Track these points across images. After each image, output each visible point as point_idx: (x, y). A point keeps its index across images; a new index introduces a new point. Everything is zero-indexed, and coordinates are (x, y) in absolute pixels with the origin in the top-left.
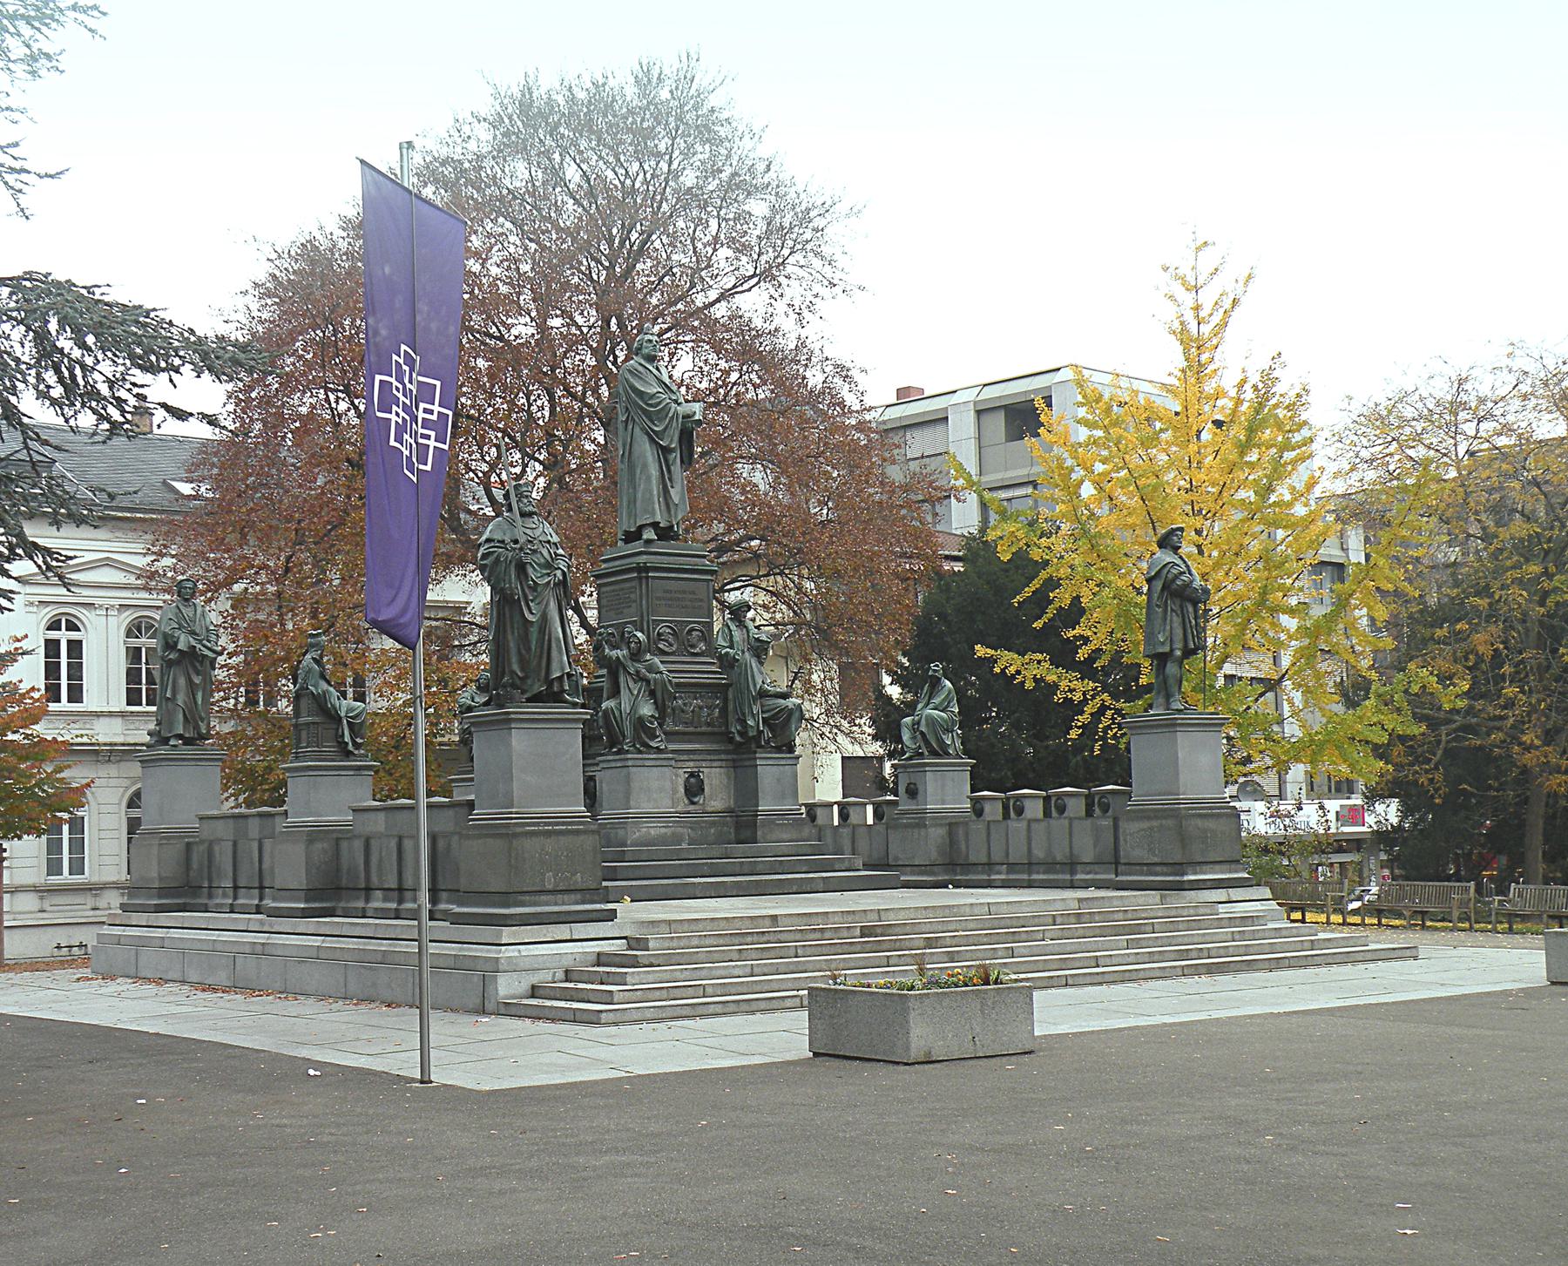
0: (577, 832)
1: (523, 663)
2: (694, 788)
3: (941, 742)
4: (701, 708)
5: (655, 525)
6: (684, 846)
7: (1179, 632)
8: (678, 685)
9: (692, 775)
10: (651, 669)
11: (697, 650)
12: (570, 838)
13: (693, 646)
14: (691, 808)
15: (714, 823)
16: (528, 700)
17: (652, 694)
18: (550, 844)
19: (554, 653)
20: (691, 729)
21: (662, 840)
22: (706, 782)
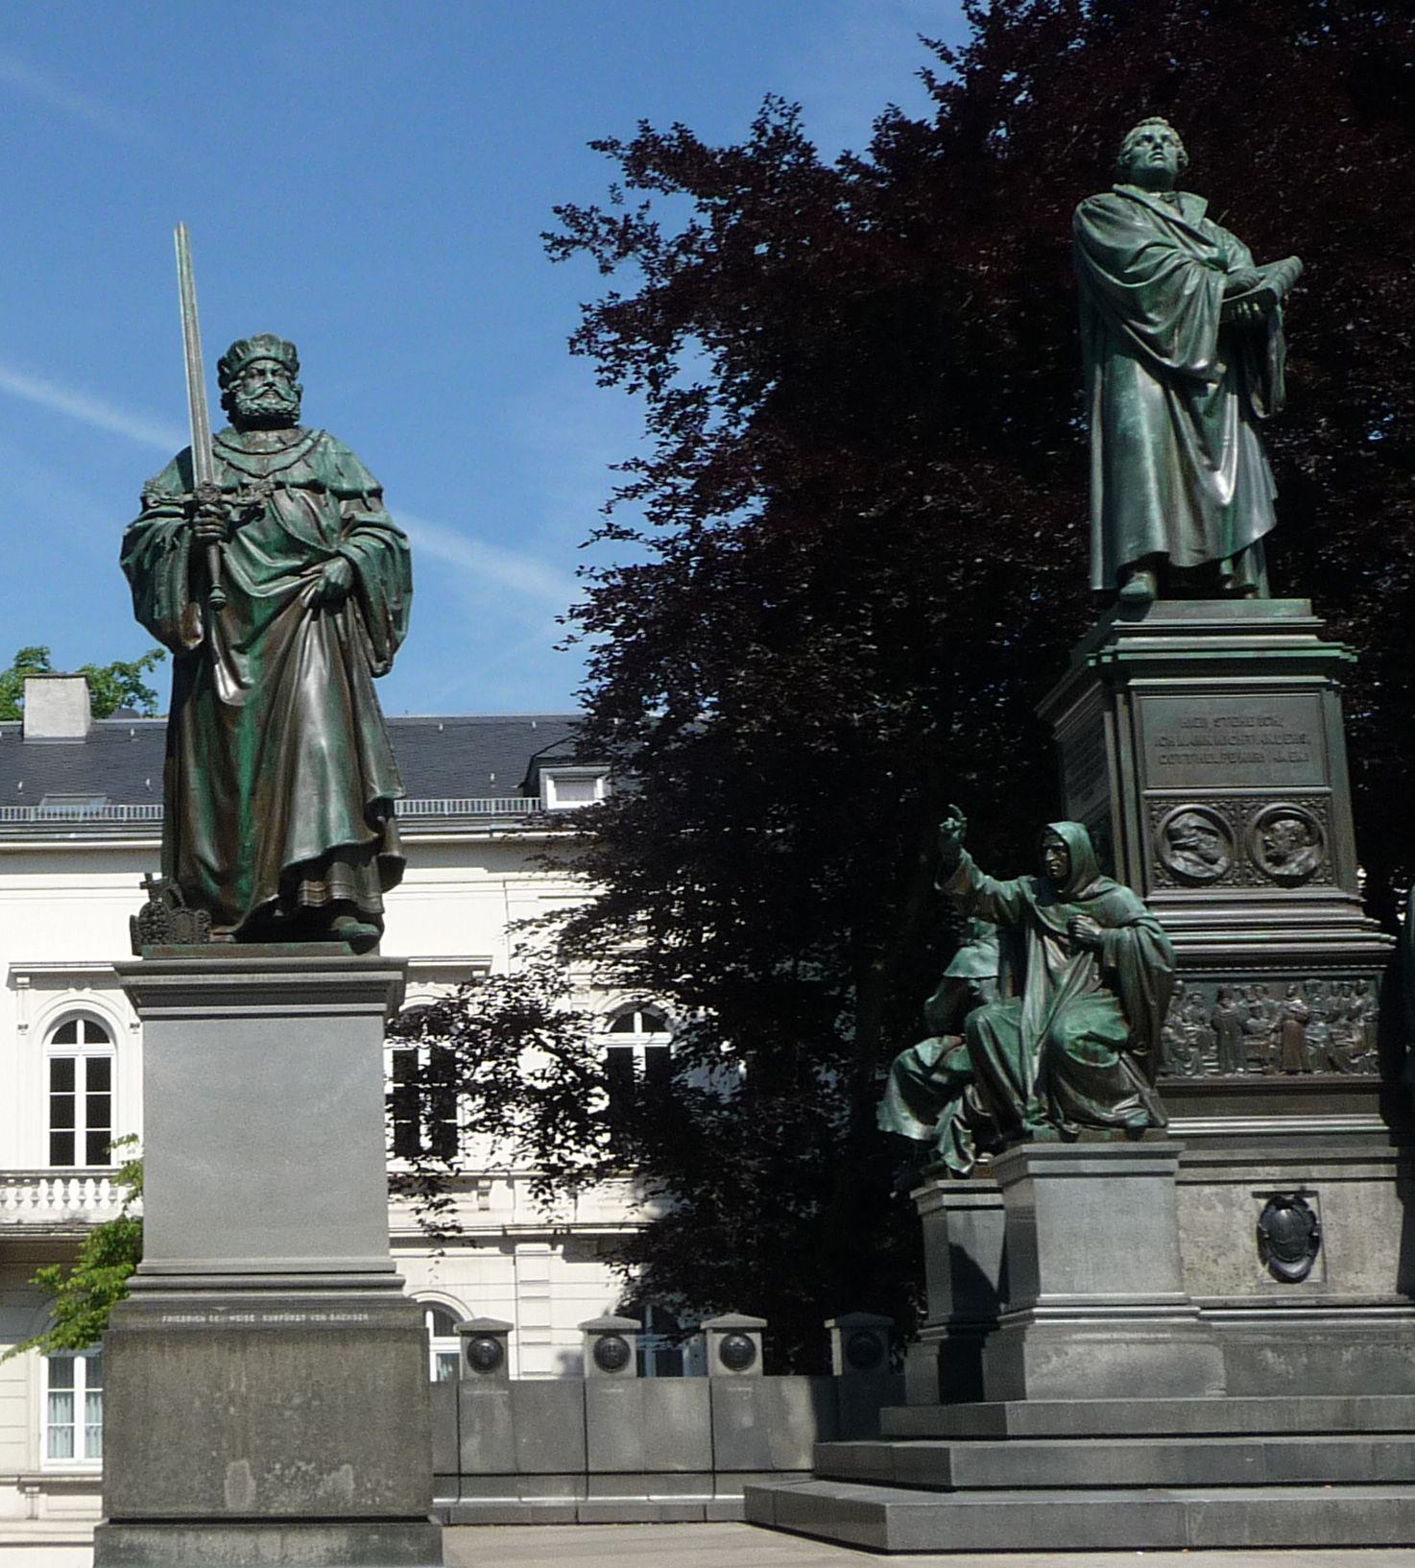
0: (344, 1334)
1: (225, 829)
2: (1288, 1239)
4: (1305, 1021)
5: (1157, 563)
6: (1213, 1394)
8: (1185, 961)
9: (1276, 1200)
10: (1109, 918)
11: (1292, 869)
12: (314, 1352)
13: (1279, 860)
14: (1283, 1292)
15: (1351, 1336)
16: (241, 937)
17: (1111, 980)
18: (241, 1371)
19: (305, 794)
20: (1279, 1077)
21: (1130, 1381)
22: (1327, 1219)
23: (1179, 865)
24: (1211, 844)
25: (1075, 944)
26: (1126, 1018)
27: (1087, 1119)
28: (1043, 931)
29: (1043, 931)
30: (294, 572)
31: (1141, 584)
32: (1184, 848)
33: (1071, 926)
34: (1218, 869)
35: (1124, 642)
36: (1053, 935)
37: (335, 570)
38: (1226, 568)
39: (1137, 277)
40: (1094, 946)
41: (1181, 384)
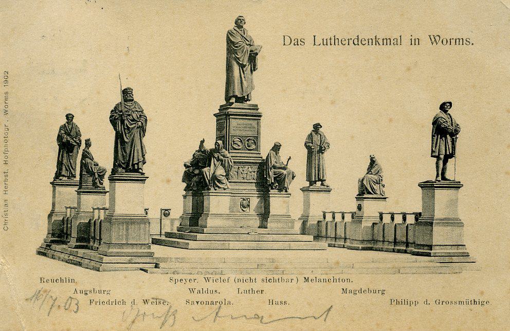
3: (373, 189)
5: (236, 97)
7: (443, 148)
23: (234, 146)
24: (240, 144)
25: (218, 160)
26: (226, 172)
27: (219, 187)
28: (214, 157)
29: (214, 157)
30: (135, 124)
31: (233, 100)
32: (236, 144)
33: (218, 157)
34: (240, 147)
35: (229, 110)
36: (216, 158)
37: (140, 123)
38: (246, 97)
39: (237, 47)
40: (222, 161)
41: (242, 66)
